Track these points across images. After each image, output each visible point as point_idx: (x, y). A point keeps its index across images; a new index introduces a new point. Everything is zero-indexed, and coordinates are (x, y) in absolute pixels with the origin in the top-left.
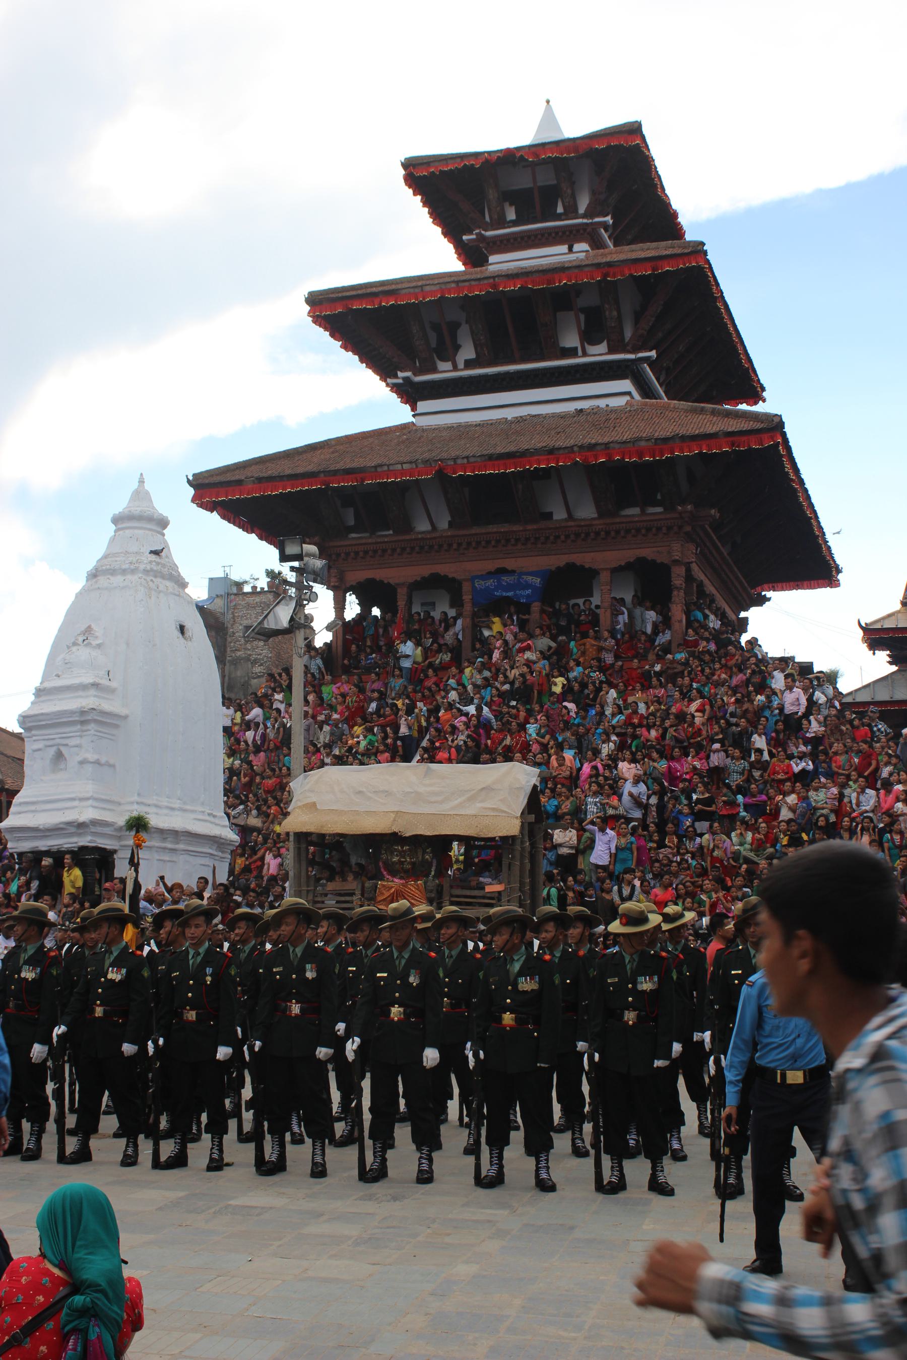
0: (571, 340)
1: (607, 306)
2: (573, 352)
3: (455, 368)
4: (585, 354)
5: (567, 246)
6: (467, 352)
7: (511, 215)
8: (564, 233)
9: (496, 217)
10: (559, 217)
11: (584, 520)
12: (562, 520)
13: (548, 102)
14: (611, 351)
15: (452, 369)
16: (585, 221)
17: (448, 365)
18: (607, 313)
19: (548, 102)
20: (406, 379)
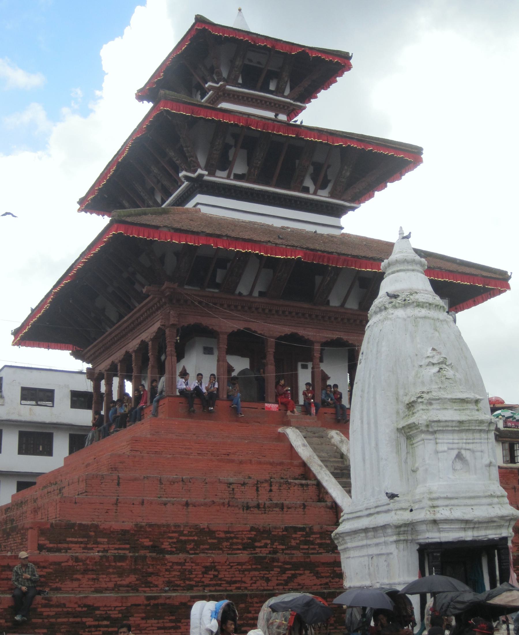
0: (308, 183)
1: (346, 167)
2: (306, 190)
3: (228, 177)
4: (315, 193)
5: (274, 114)
6: (240, 168)
7: (240, 81)
8: (284, 106)
9: (233, 77)
10: (271, 92)
11: (351, 309)
12: (335, 307)
13: (240, 10)
14: (332, 195)
15: (225, 176)
16: (292, 102)
17: (225, 174)
18: (344, 172)
19: (240, 10)
20: (201, 176)
